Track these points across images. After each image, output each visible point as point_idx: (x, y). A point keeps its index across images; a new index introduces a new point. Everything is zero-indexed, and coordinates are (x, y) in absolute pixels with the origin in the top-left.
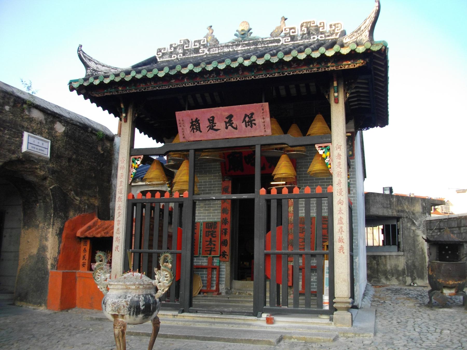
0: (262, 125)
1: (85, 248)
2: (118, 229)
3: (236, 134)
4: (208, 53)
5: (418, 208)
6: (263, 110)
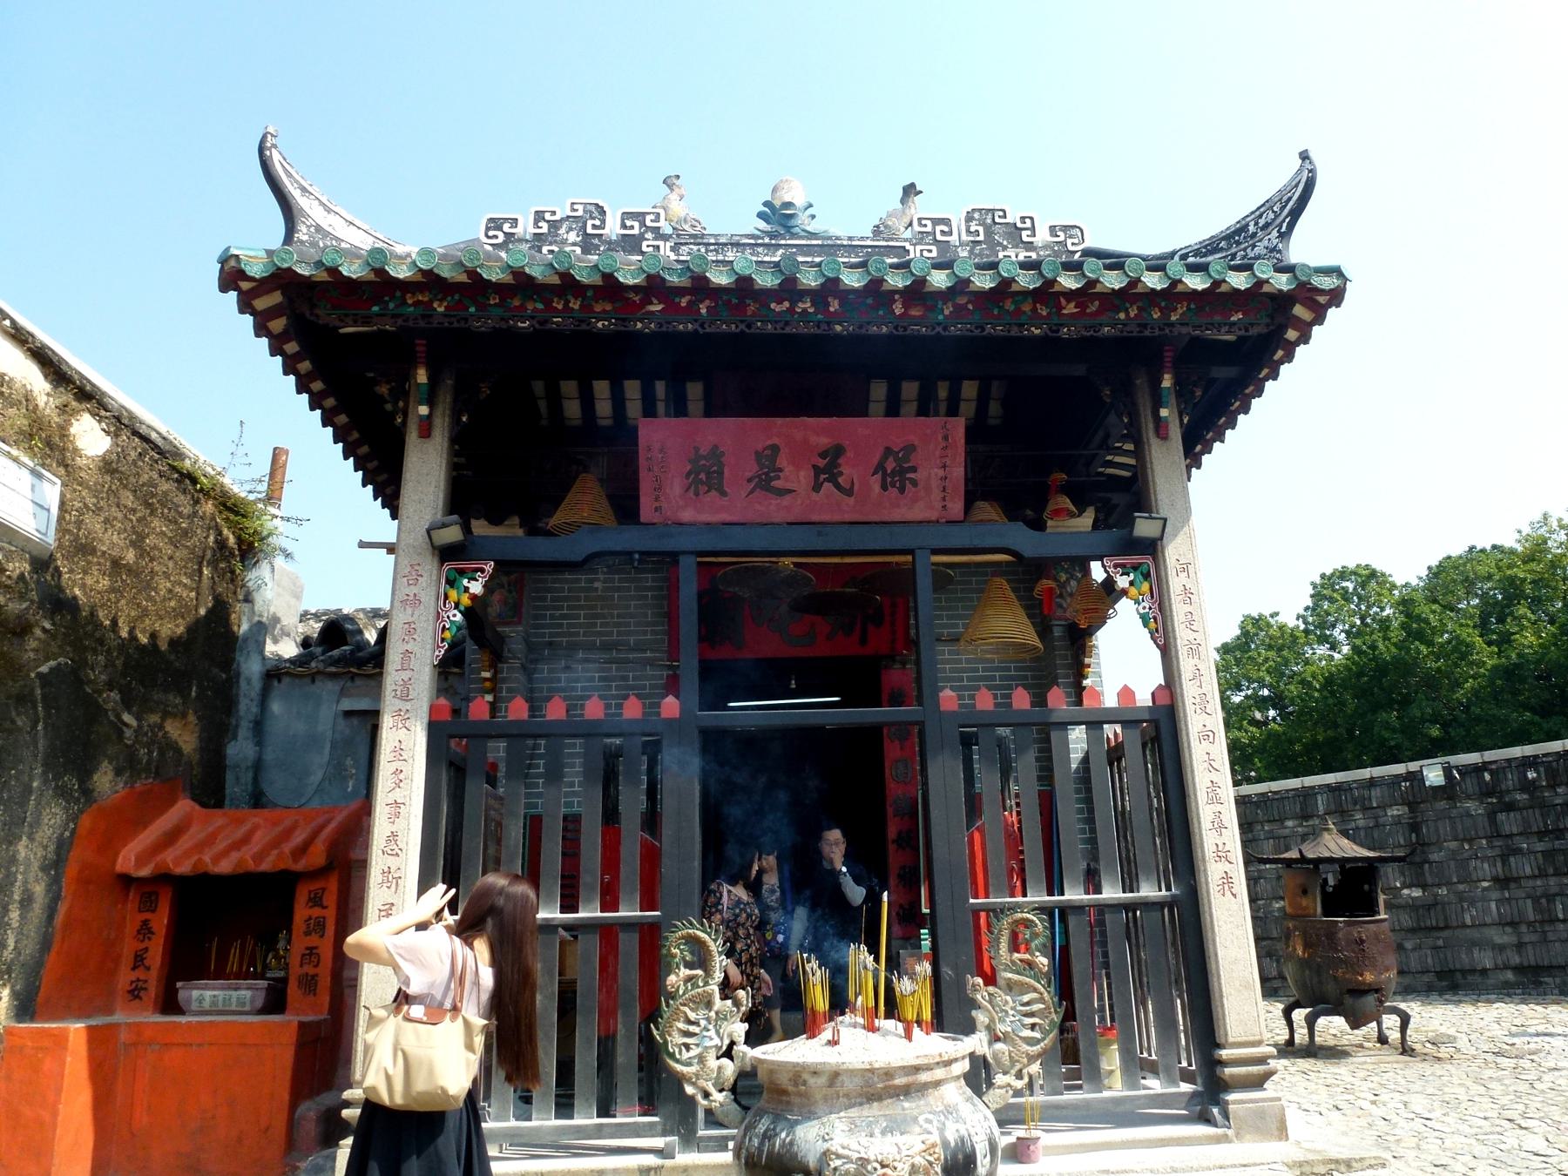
0: (934, 483)
1: (145, 922)
6: (946, 438)
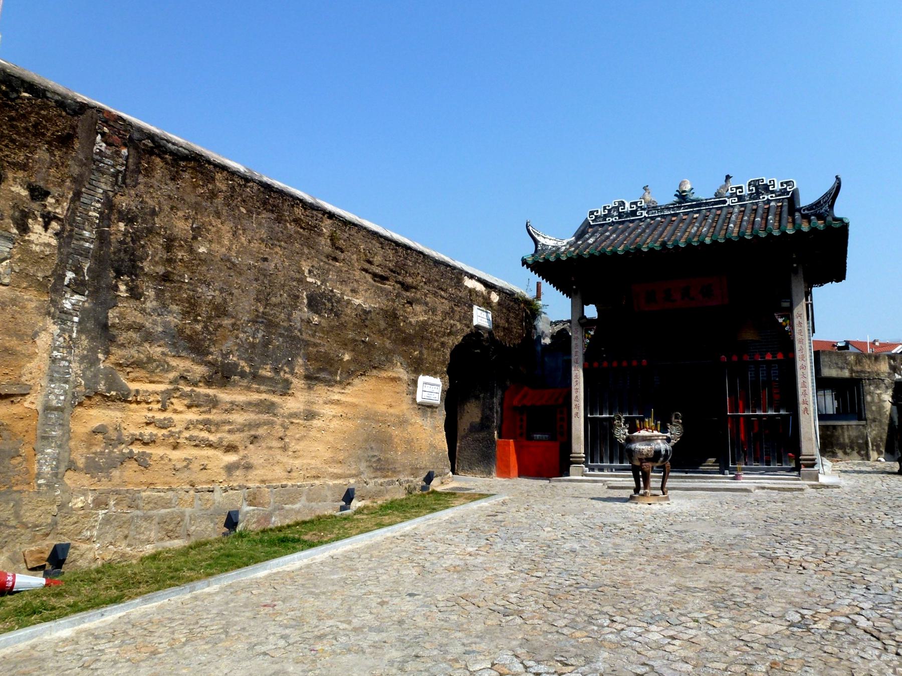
5: (884, 367)
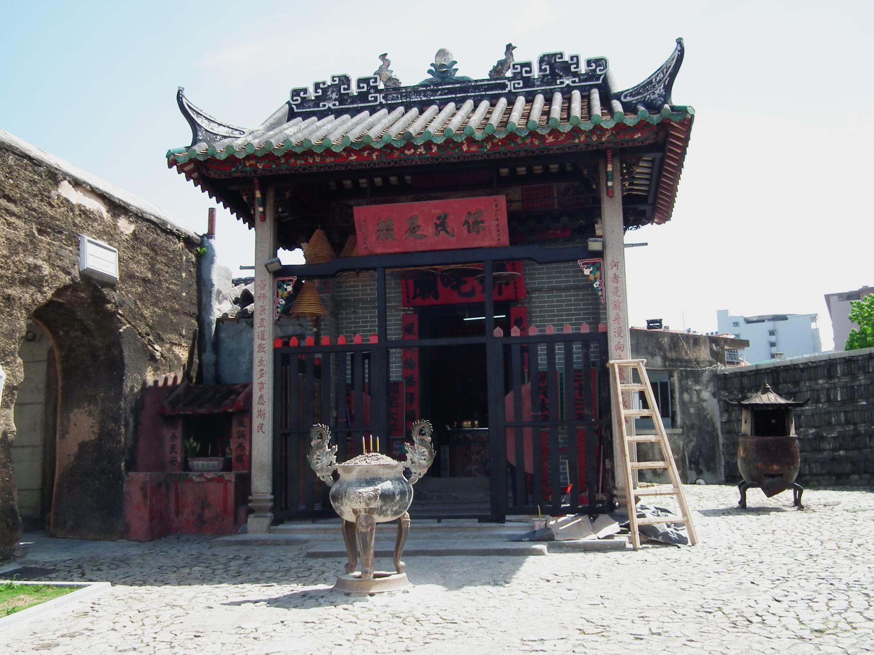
0: (493, 228)
2: (261, 397)
3: (452, 243)
4: (384, 102)
6: (497, 206)
